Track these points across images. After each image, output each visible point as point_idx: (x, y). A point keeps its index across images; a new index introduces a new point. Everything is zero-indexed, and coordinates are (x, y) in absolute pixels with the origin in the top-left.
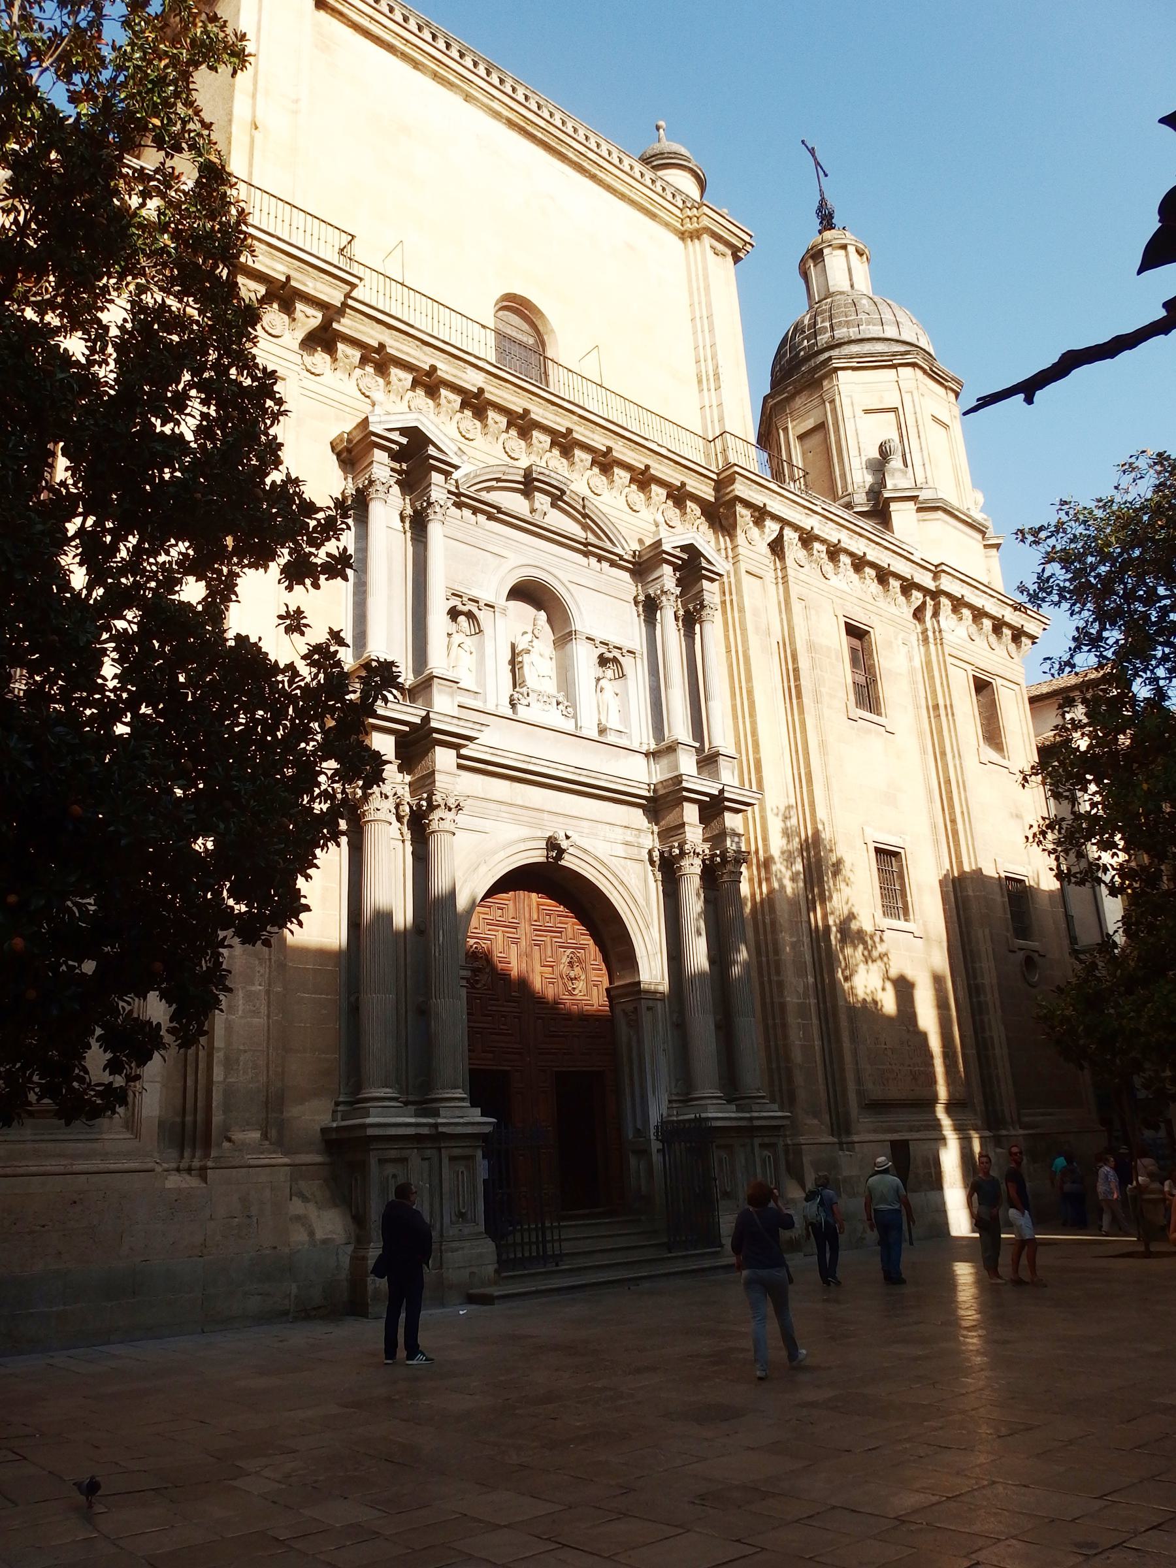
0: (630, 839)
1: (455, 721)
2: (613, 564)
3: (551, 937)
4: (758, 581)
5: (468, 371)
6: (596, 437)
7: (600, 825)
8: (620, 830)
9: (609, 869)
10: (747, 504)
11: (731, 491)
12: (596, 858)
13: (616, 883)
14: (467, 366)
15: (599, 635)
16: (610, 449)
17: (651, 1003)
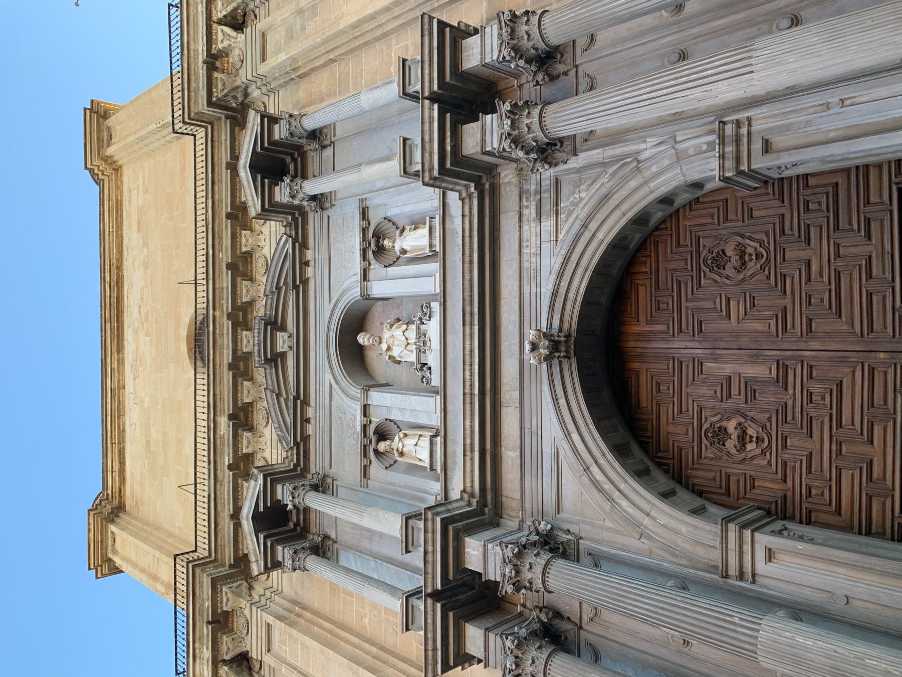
0: (533, 211)
1: (430, 557)
2: (304, 246)
3: (687, 301)
4: (269, 38)
5: (222, 433)
6: (225, 285)
7: (526, 265)
8: (526, 227)
9: (570, 252)
10: (210, 84)
11: (209, 111)
12: (560, 275)
13: (587, 235)
14: (218, 436)
15: (357, 264)
16: (229, 266)
17: (757, 146)
